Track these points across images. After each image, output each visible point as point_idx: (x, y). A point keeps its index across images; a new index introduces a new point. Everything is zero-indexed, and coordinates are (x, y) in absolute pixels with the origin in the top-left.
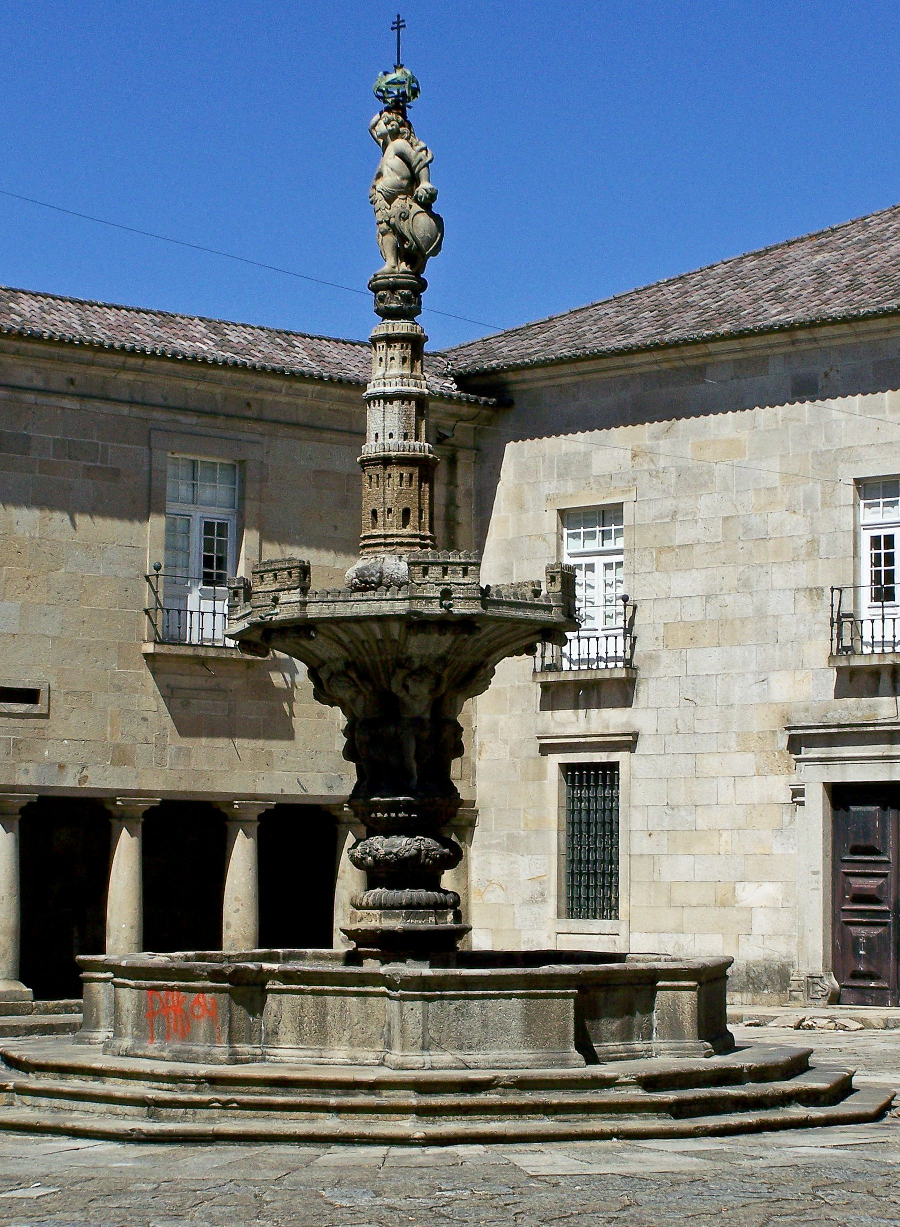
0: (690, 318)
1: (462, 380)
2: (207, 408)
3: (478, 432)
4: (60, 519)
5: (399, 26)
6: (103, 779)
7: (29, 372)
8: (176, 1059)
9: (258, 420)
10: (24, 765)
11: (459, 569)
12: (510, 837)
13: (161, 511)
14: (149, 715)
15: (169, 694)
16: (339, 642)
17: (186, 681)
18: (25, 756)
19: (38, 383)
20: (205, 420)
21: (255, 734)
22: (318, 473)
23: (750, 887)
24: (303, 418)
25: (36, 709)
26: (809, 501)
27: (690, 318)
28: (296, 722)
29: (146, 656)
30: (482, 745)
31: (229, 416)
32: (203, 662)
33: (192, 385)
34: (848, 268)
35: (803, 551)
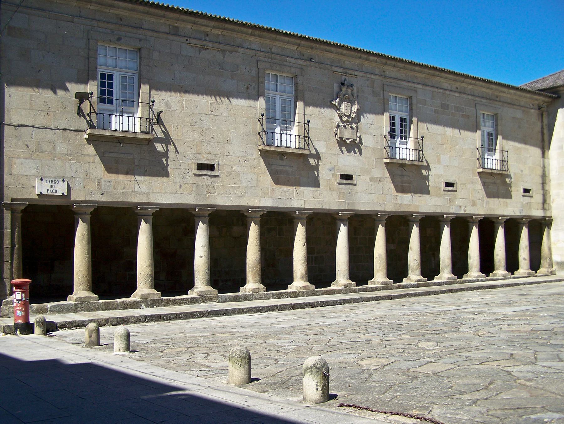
2: (488, 97)
3: (547, 106)
4: (456, 131)
6: (470, 210)
7: (447, 85)
9: (499, 101)
13: (480, 129)
15: (484, 184)
17: (487, 180)
18: (452, 204)
19: (449, 88)
20: (488, 101)
21: (503, 198)
22: (513, 118)
24: (509, 101)
25: (454, 189)
28: (512, 193)
29: (479, 173)
30: (553, 200)
31: (493, 100)
32: (491, 174)
33: (484, 90)
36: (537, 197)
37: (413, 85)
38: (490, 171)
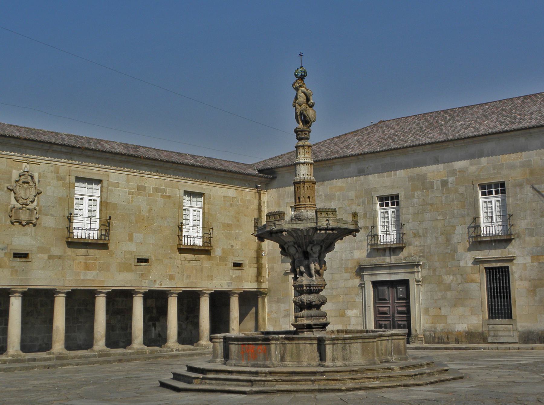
0: (323, 154)
1: (260, 171)
5: (301, 55)
8: (253, 366)
10: (144, 281)
11: (331, 213)
12: (278, 298)
14: (179, 266)
16: (293, 236)
22: (224, 196)
23: (349, 311)
26: (363, 203)
27: (323, 154)
34: (366, 140)
35: (362, 216)
36: (250, 271)
37: (105, 170)
38: (191, 247)
